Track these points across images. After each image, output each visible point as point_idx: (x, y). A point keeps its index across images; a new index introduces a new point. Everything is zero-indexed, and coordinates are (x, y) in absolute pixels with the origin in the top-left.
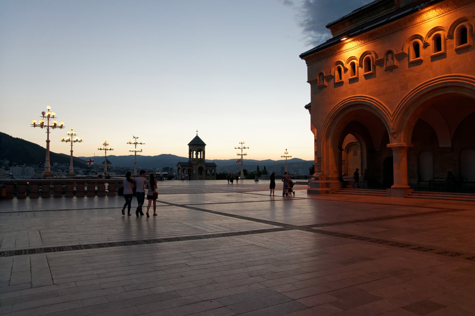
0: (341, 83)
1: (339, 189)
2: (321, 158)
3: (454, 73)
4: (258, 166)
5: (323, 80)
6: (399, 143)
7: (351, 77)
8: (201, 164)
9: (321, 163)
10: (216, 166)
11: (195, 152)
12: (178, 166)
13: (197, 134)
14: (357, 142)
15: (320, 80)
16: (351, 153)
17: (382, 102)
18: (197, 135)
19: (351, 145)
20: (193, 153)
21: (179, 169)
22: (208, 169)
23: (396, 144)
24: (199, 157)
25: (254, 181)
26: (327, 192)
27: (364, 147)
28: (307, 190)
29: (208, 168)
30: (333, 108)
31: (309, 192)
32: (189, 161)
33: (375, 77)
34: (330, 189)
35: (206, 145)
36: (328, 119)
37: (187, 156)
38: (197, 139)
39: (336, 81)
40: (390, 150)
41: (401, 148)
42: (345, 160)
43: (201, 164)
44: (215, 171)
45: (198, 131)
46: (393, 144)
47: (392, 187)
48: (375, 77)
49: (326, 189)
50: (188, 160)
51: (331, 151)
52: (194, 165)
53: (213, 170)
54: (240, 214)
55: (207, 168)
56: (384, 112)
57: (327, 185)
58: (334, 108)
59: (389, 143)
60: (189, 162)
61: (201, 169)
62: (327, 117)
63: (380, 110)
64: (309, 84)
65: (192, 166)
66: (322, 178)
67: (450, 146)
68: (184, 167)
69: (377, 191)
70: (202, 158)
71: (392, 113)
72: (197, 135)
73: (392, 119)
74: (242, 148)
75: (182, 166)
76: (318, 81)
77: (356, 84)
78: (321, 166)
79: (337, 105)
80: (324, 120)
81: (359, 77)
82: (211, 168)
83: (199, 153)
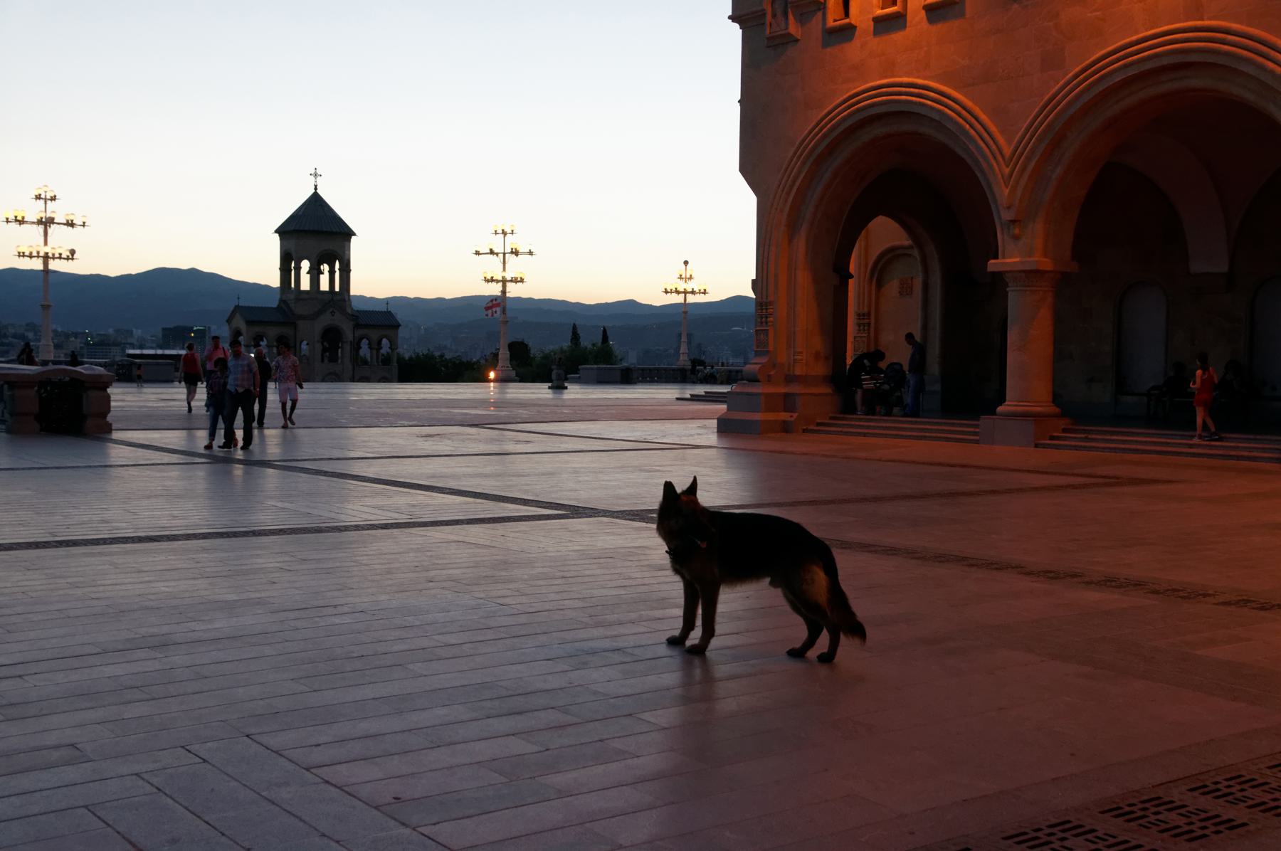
0: (846, 32)
1: (831, 418)
2: (771, 303)
3: (1210, 19)
4: (575, 327)
5: (785, 14)
6: (1024, 260)
7: (882, 9)
8: (333, 313)
9: (767, 323)
10: (397, 326)
11: (305, 265)
13: (316, 186)
14: (910, 247)
15: (774, 16)
16: (892, 287)
17: (977, 111)
18: (316, 189)
19: (890, 257)
20: (298, 269)
21: (237, 333)
22: (361, 339)
23: (1018, 260)
24: (324, 285)
25: (549, 388)
26: (786, 428)
27: (936, 266)
28: (716, 421)
29: (366, 331)
30: (814, 123)
31: (725, 427)
32: (282, 301)
33: (962, 15)
34: (797, 414)
35: (354, 234)
36: (796, 163)
37: (274, 280)
38: (316, 204)
39: (831, 23)
40: (999, 277)
41: (1031, 276)
42: (869, 314)
43: (333, 313)
44: (393, 346)
45: (319, 172)
46: (1008, 260)
47: (1000, 409)
48: (962, 15)
49: (784, 416)
50: (278, 297)
51: (803, 278)
53: (385, 341)
54: (452, 484)
55: (360, 332)
56: (982, 145)
57: (787, 402)
58: (818, 124)
59: (997, 258)
60: (279, 308)
61: (331, 337)
62: (795, 153)
63: (971, 138)
64: (737, 26)
66: (769, 376)
67: (1224, 268)
68: (257, 329)
69: (953, 425)
70: (337, 289)
71: (1007, 151)
72: (316, 189)
73: (1007, 171)
74: (504, 254)
75: (249, 323)
76: (769, 17)
77: (897, 37)
78: (767, 335)
79: (829, 113)
80: (784, 167)
81: (908, 11)
82: (374, 335)
83: (325, 268)
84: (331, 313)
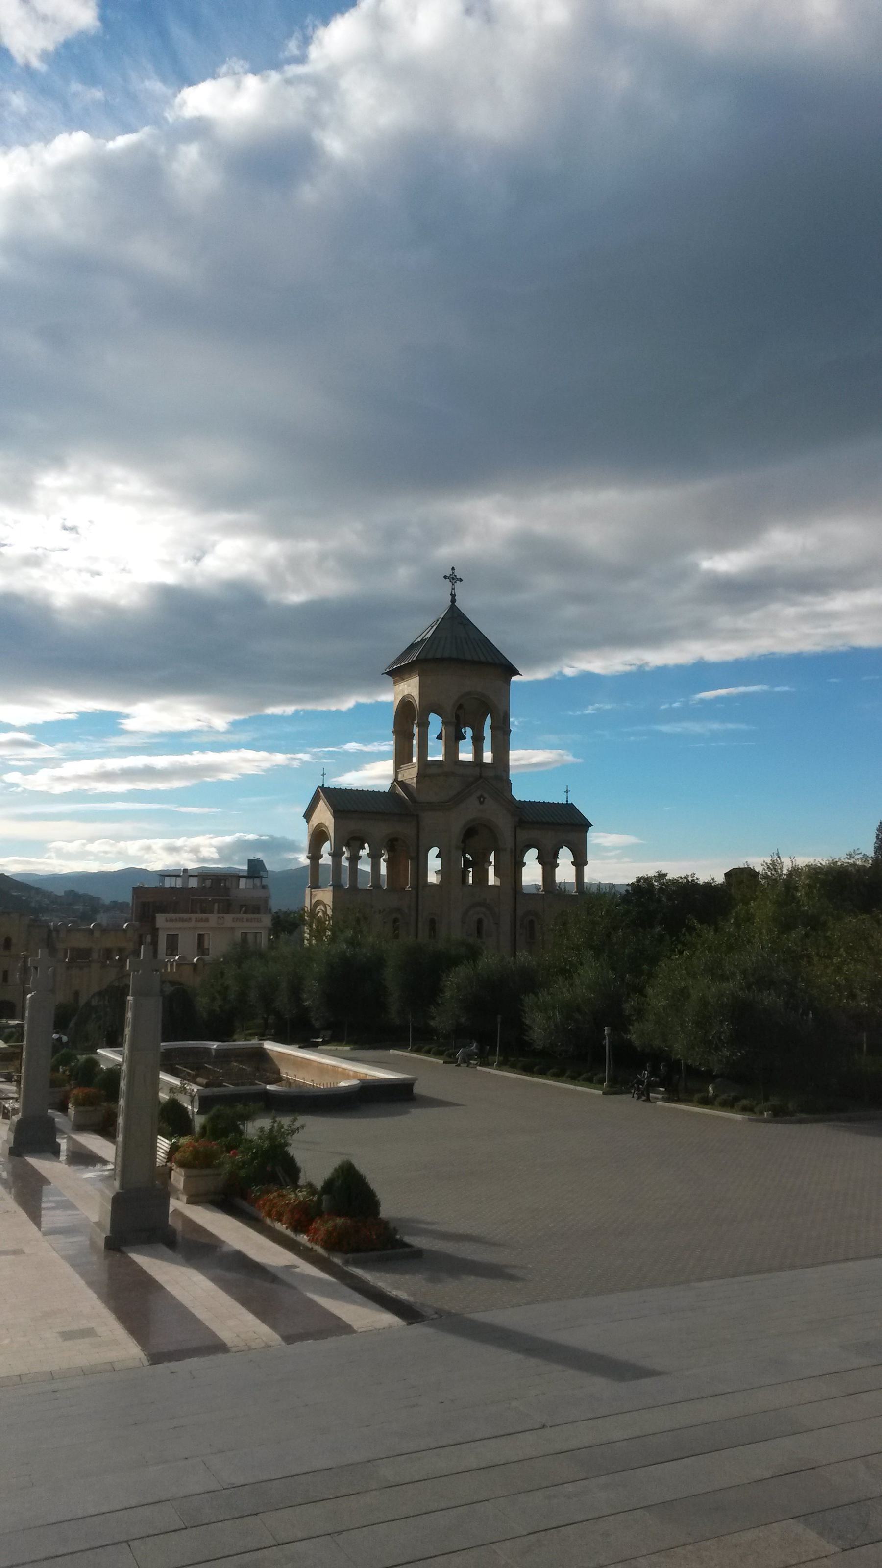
8: (481, 800)
12: (316, 819)
13: (453, 596)
18: (453, 601)
35: (516, 672)
43: (481, 800)
52: (432, 807)
55: (524, 835)
65: (417, 816)
72: (453, 601)
75: (338, 813)
84: (479, 798)
